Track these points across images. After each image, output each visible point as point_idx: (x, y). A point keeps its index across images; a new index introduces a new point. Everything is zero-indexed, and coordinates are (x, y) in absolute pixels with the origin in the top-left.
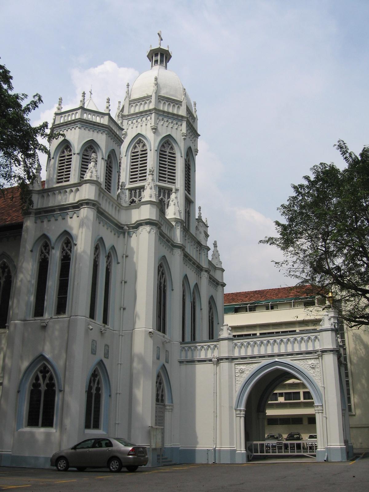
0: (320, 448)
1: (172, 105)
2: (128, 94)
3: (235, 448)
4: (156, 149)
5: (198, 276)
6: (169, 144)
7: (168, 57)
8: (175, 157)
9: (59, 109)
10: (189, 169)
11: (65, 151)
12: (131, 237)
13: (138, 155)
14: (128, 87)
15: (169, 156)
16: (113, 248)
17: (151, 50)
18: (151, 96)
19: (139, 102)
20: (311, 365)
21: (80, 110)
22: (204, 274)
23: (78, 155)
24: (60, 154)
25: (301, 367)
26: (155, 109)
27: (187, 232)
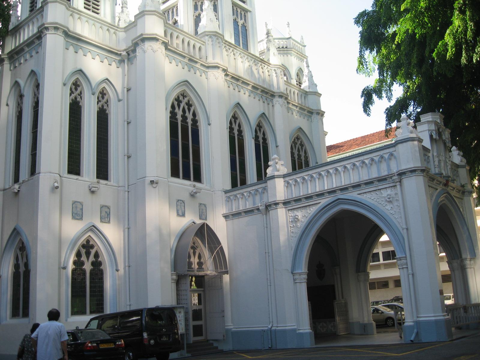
0: (409, 322)
3: (295, 327)
20: (386, 198)
22: (277, 101)
25: (372, 202)
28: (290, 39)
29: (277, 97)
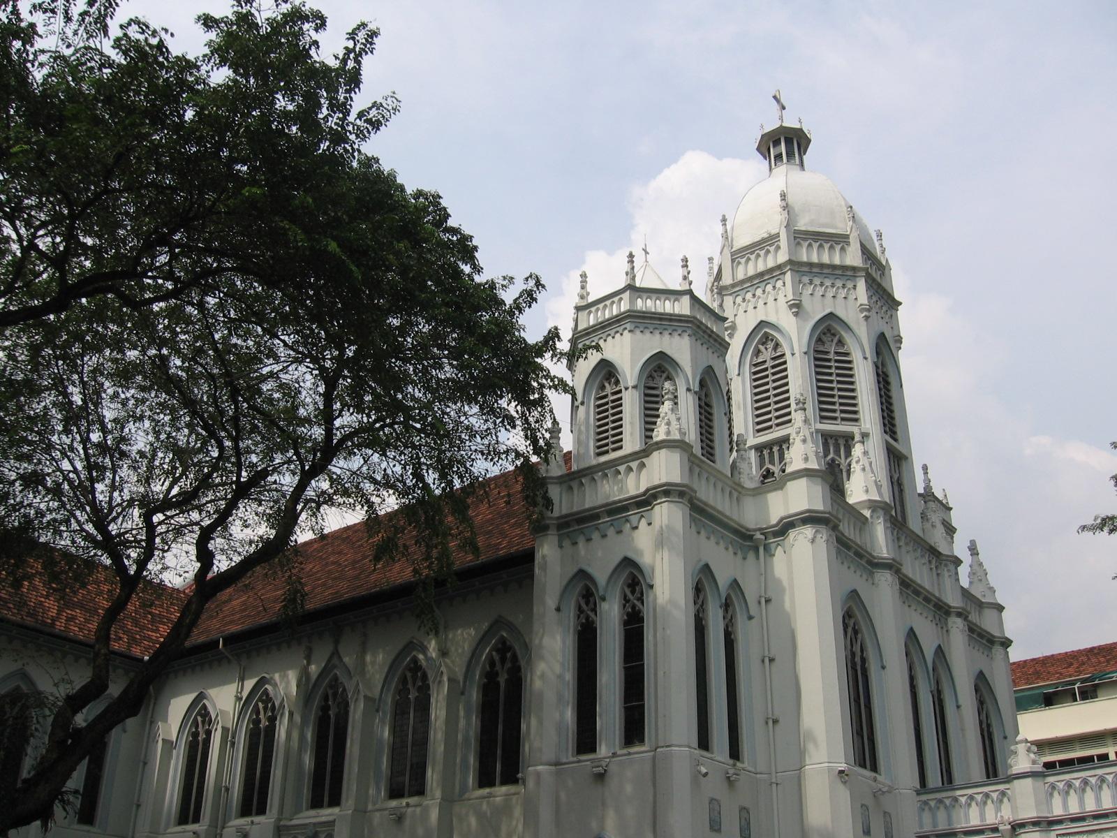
1: (827, 246)
2: (727, 238)
4: (805, 350)
5: (942, 628)
6: (834, 335)
7: (803, 143)
8: (850, 362)
9: (582, 297)
10: (887, 383)
11: (607, 385)
12: (774, 555)
13: (766, 369)
14: (725, 225)
15: (837, 361)
16: (735, 584)
17: (763, 136)
18: (778, 235)
19: (752, 253)
21: (628, 292)
22: (954, 622)
23: (634, 390)
24: (597, 393)
26: (790, 262)
27: (900, 529)
29: (953, 615)
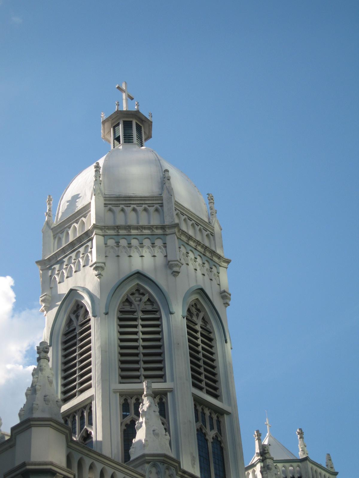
28: (305, 462)
